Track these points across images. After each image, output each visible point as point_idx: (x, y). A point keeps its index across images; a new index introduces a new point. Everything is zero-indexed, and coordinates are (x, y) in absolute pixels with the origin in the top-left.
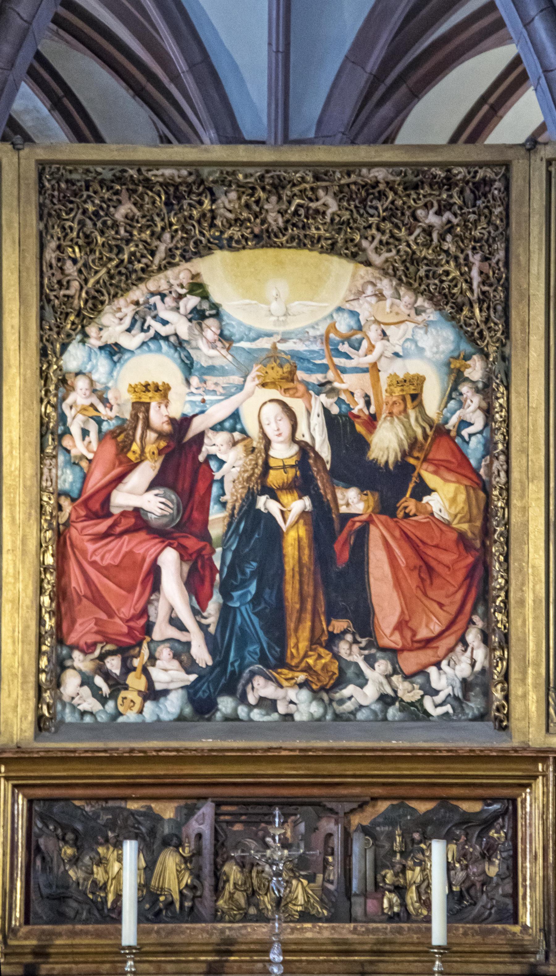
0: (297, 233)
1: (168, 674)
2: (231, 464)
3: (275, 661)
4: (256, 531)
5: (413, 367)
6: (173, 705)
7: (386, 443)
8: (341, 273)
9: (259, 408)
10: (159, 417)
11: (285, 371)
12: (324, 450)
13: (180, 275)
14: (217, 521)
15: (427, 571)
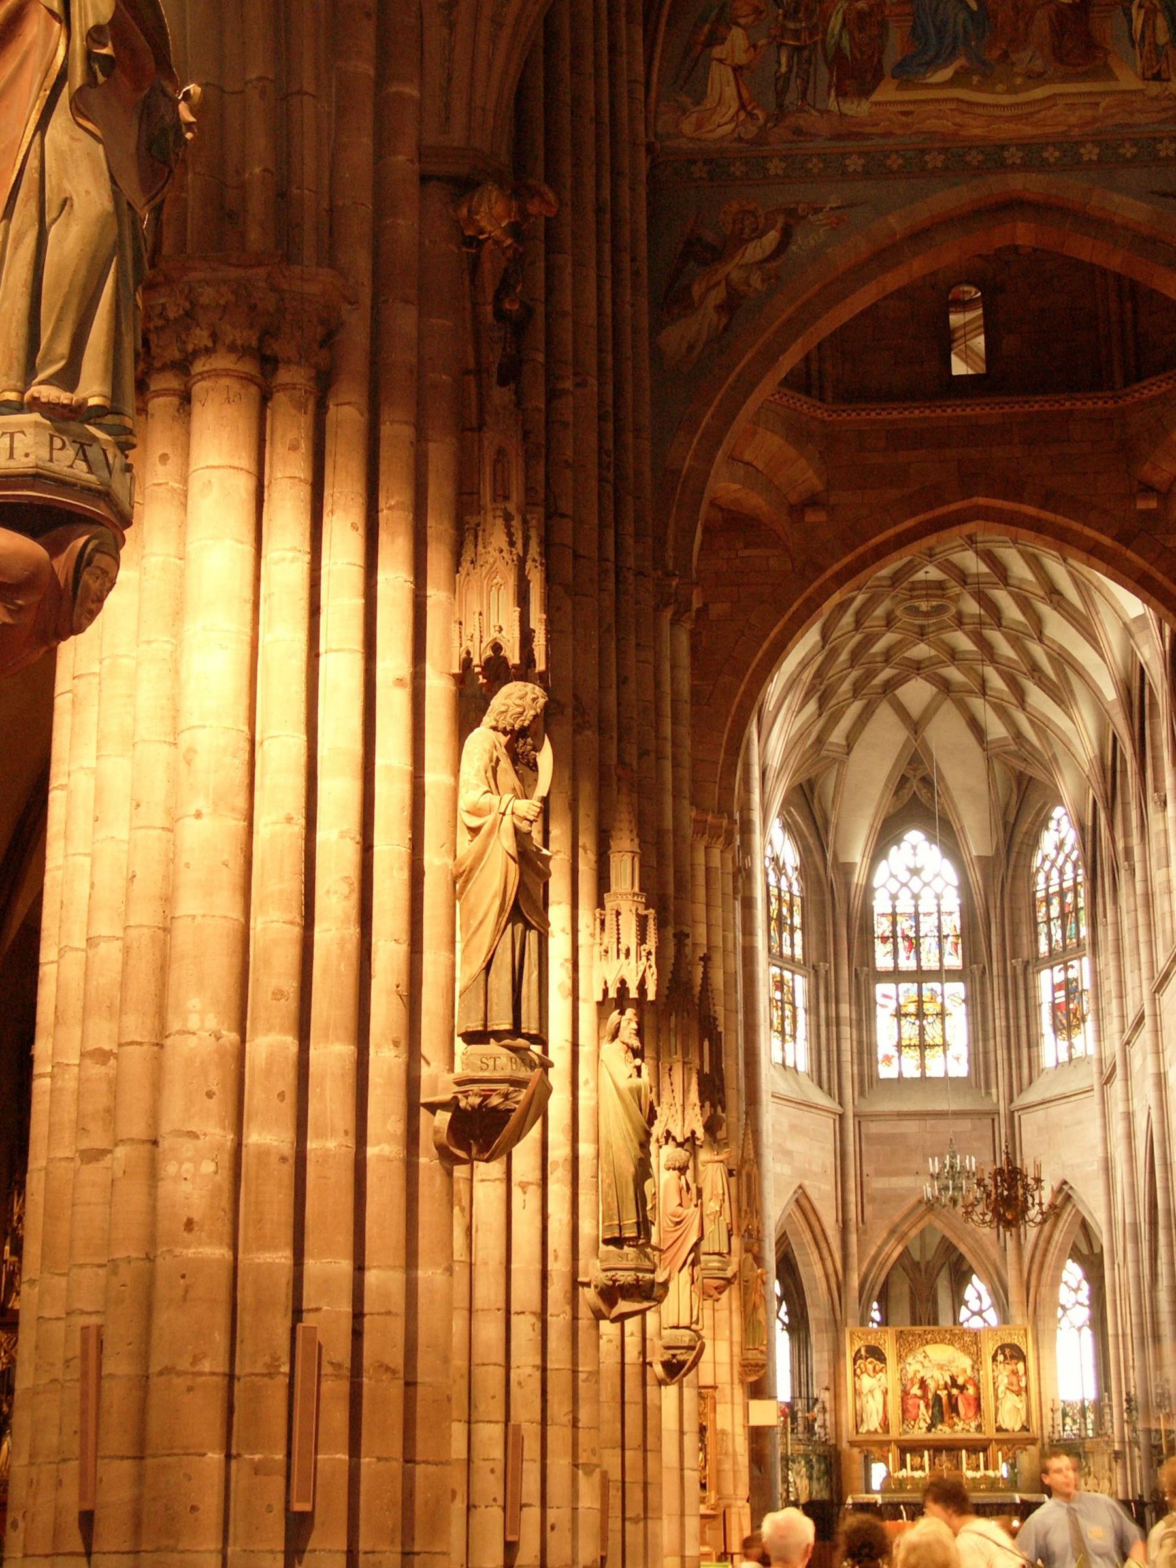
0: (942, 1341)
1: (923, 1425)
2: (932, 1385)
3: (942, 1421)
4: (937, 1398)
5: (963, 1366)
6: (924, 1430)
7: (960, 1381)
8: (950, 1349)
9: (937, 1374)
10: (919, 1376)
11: (941, 1367)
12: (949, 1382)
13: (921, 1350)
14: (930, 1396)
15: (969, 1404)
